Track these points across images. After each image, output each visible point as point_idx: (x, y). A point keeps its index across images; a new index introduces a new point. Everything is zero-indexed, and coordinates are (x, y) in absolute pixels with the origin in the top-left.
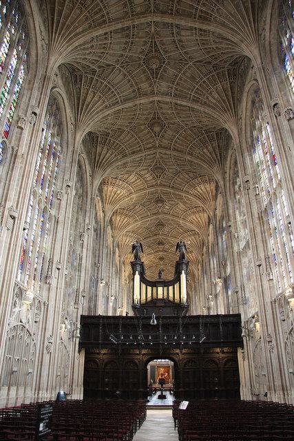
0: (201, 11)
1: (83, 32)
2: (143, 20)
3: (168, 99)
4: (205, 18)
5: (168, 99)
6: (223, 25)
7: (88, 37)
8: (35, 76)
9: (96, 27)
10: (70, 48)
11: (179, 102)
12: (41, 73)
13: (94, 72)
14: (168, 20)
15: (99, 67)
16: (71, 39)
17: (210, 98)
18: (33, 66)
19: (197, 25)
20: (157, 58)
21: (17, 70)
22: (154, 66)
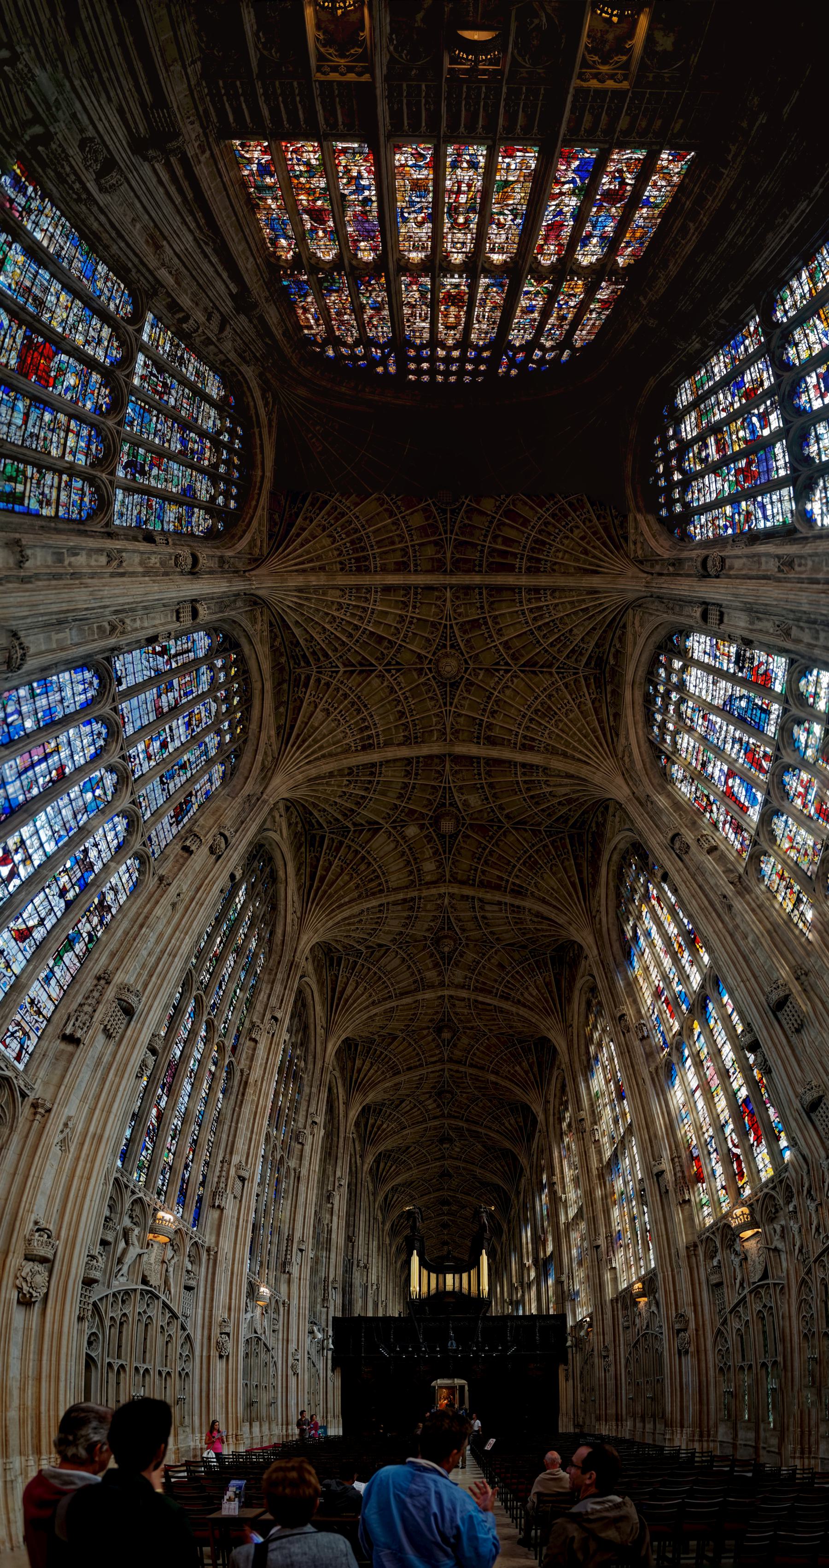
0: (514, 884)
1: (350, 902)
2: (434, 891)
3: (464, 994)
4: (518, 892)
5: (464, 994)
6: (543, 901)
7: (356, 910)
8: (279, 962)
9: (367, 896)
10: (330, 923)
11: (480, 999)
12: (286, 958)
13: (359, 953)
14: (468, 891)
15: (367, 947)
16: (333, 910)
17: (526, 995)
18: (277, 948)
19: (508, 899)
20: (450, 938)
21: (255, 955)
22: (446, 949)
